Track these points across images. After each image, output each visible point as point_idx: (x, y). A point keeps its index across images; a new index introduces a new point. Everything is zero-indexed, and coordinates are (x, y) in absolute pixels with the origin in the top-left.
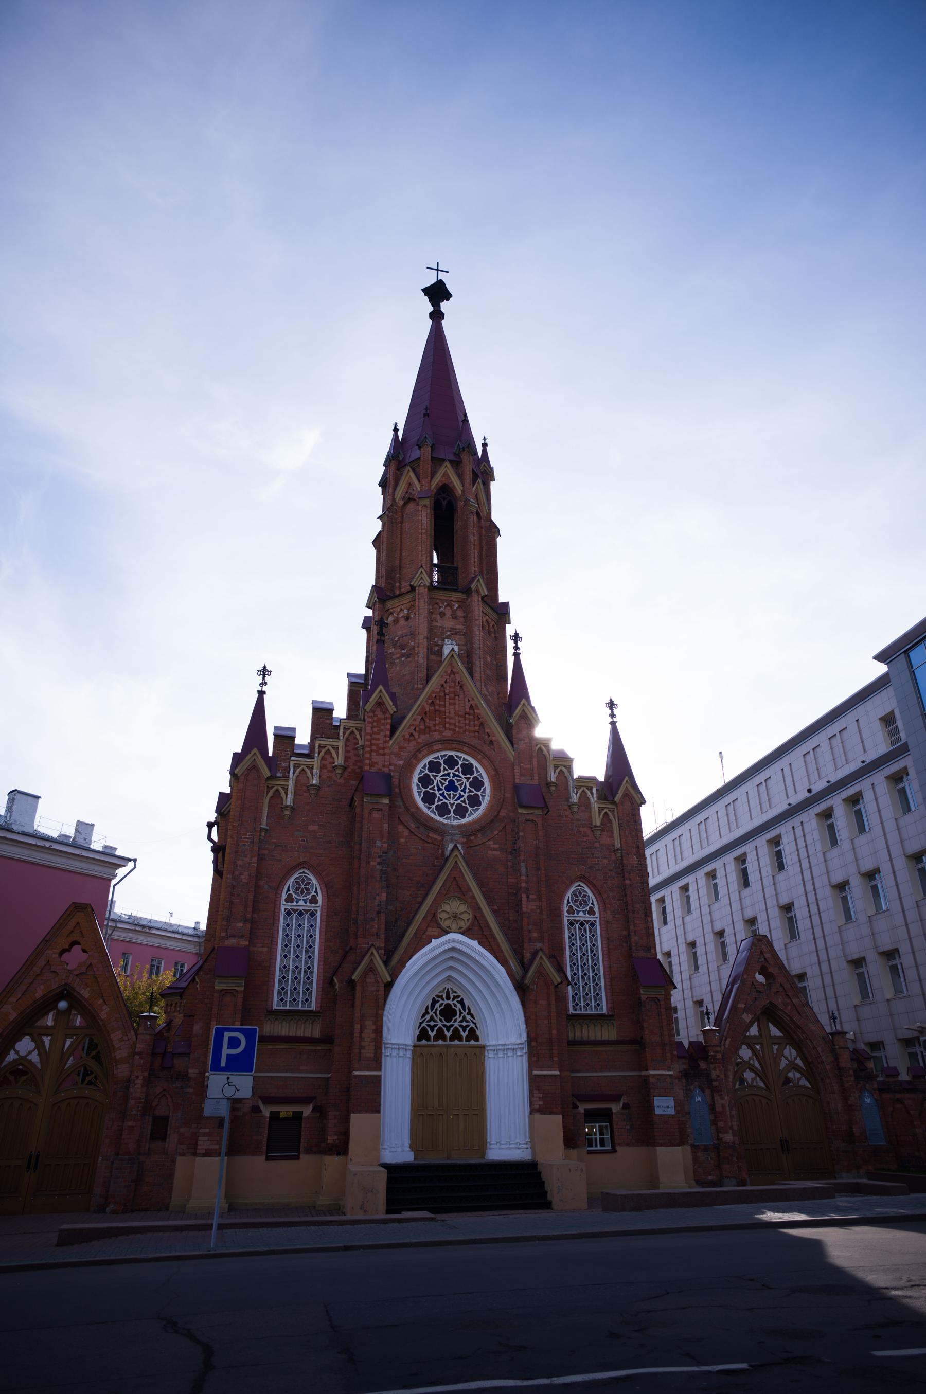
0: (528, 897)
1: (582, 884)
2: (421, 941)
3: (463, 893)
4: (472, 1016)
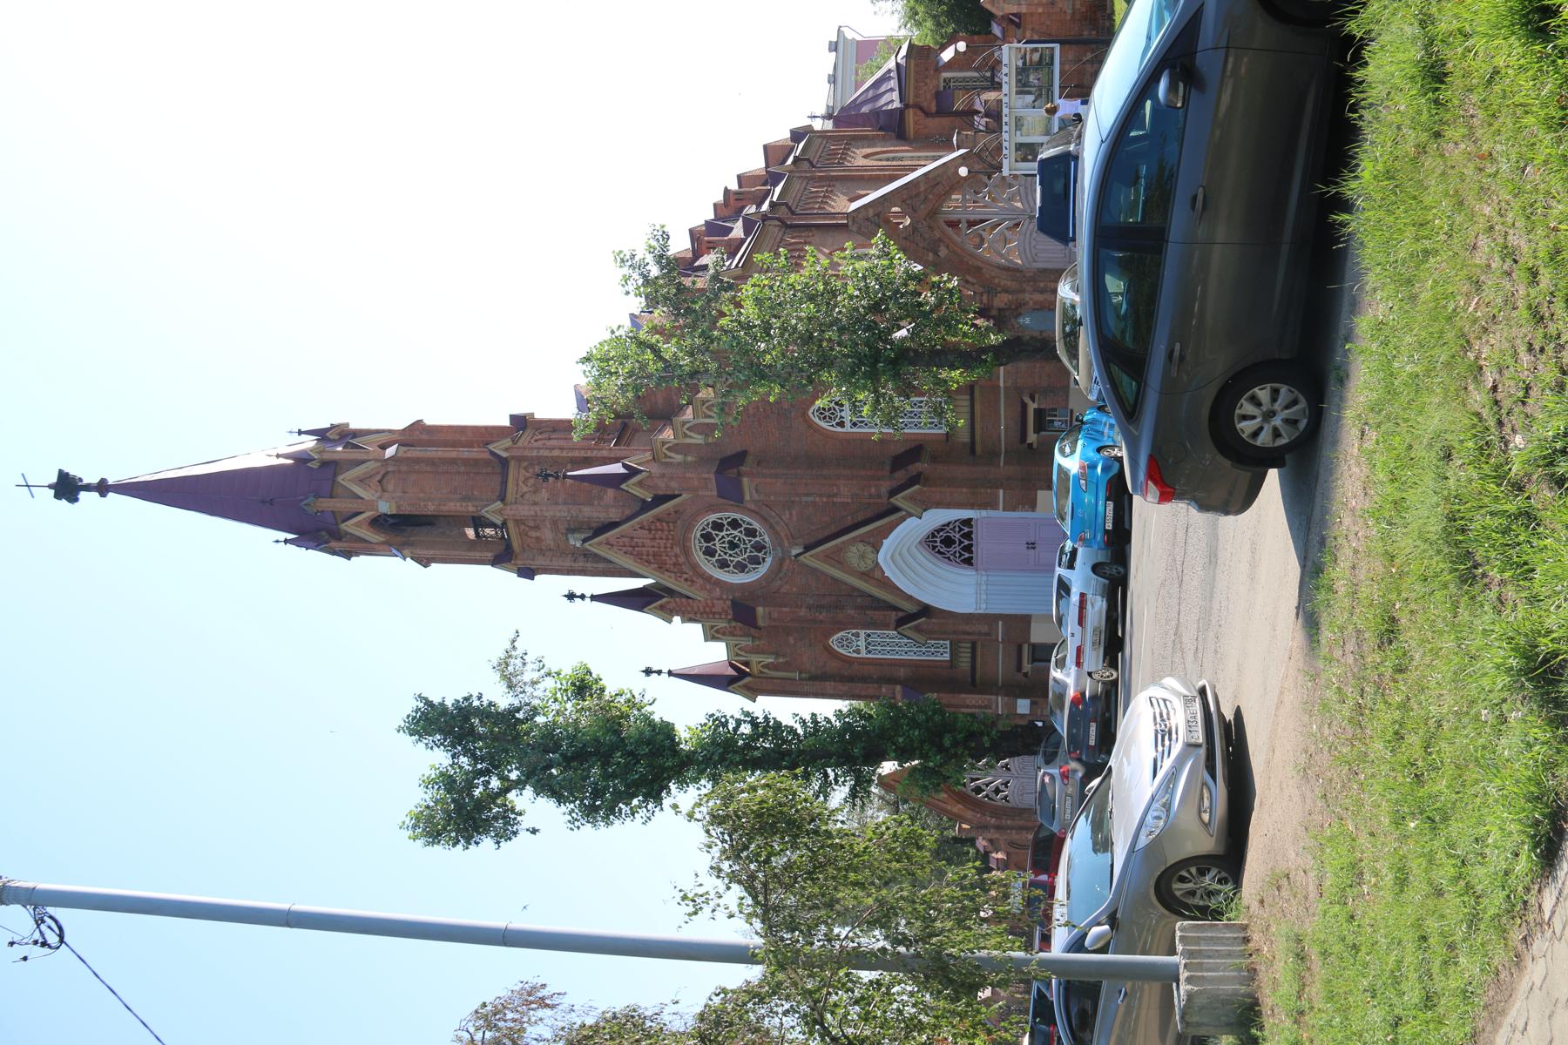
0: (835, 495)
2: (887, 584)
4: (949, 523)
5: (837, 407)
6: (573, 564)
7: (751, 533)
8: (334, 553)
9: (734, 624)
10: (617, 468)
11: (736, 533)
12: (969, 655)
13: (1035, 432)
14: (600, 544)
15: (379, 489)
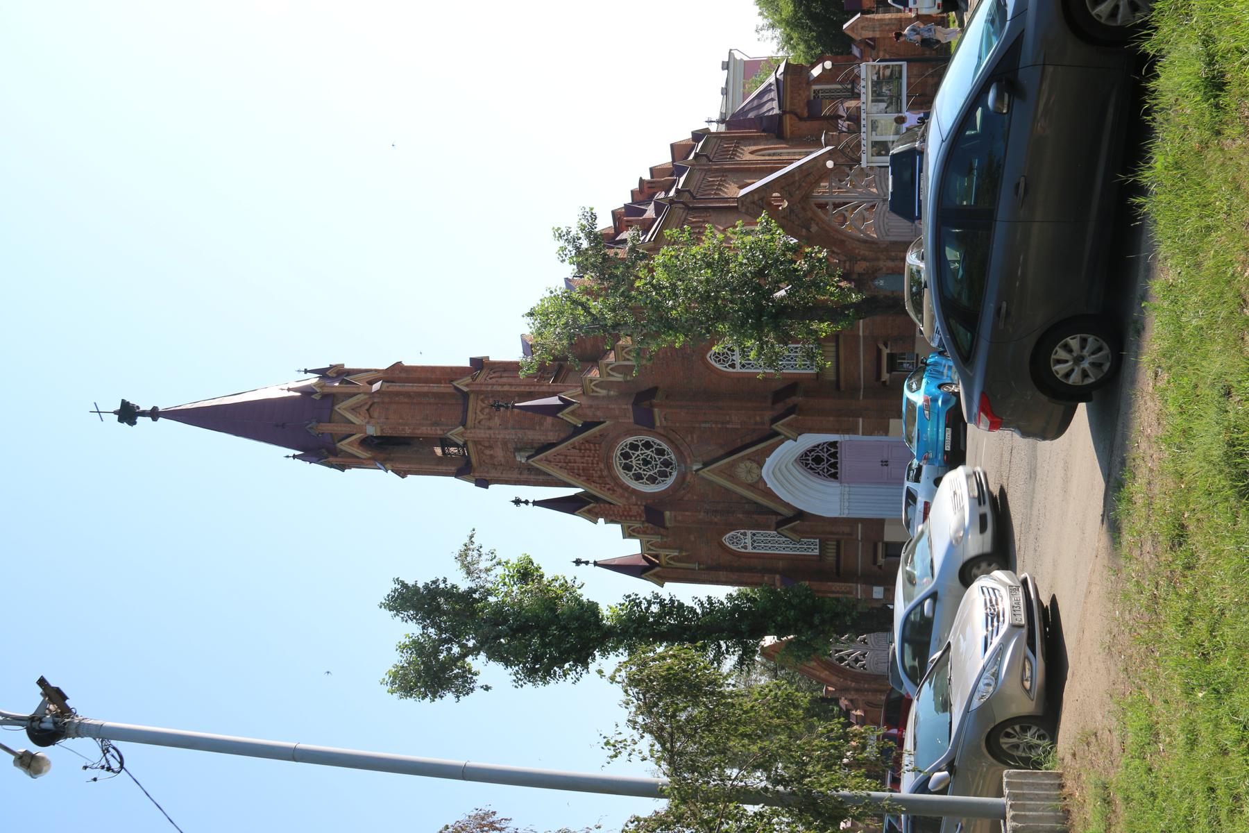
0: (728, 422)
1: (709, 355)
2: (769, 494)
3: (733, 465)
4: (819, 445)
5: (729, 352)
6: (519, 476)
7: (661, 452)
8: (331, 466)
9: (646, 525)
10: (554, 401)
11: (648, 452)
12: (835, 551)
13: (888, 372)
14: (541, 460)
15: (367, 415)
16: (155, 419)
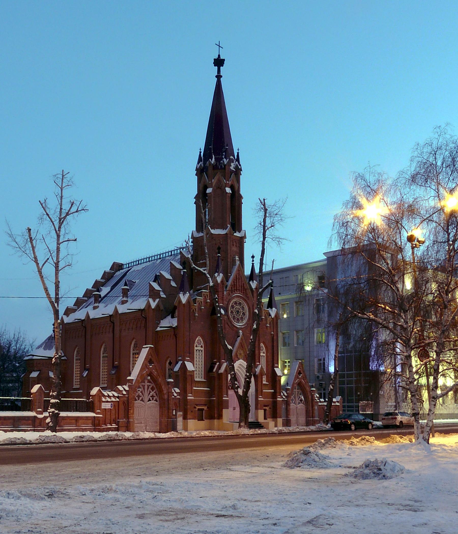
16: (216, 77)
